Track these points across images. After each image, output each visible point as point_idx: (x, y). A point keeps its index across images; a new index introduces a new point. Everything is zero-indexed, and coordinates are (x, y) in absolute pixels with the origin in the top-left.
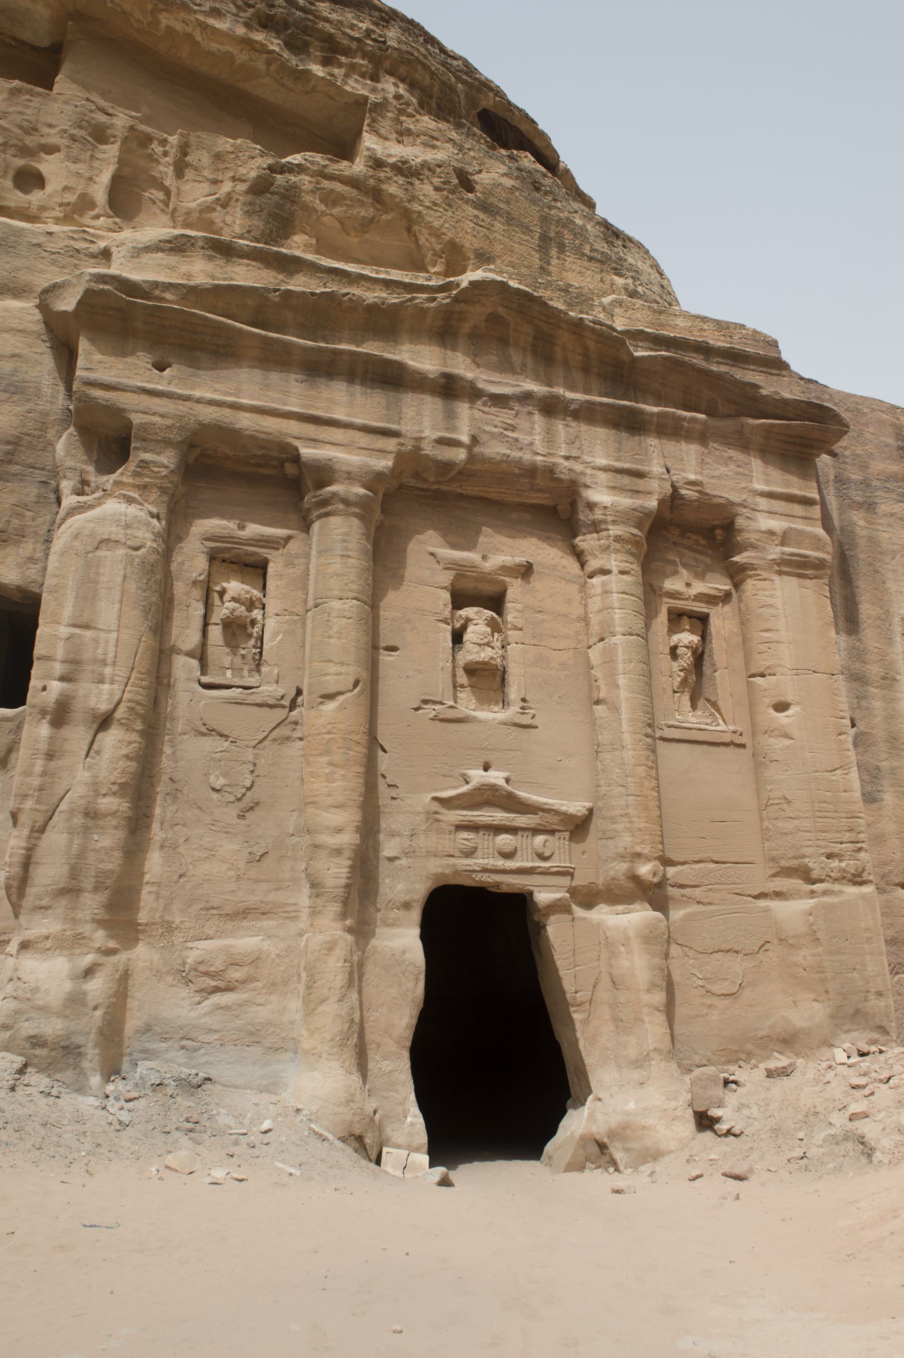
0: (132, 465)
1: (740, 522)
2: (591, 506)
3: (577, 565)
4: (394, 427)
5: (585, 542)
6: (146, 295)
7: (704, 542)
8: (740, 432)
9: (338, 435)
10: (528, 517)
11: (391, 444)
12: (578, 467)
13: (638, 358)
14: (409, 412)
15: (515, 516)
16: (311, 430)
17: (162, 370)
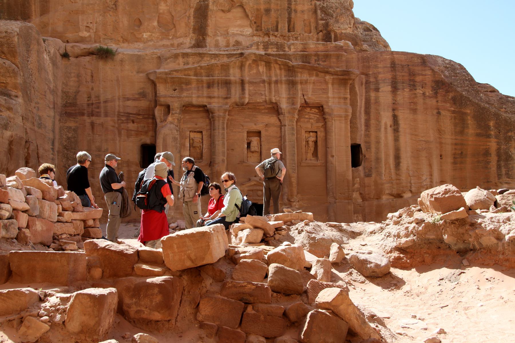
0: (170, 115)
1: (325, 106)
2: (281, 108)
3: (279, 123)
4: (229, 96)
5: (281, 117)
6: (170, 74)
7: (317, 111)
8: (325, 81)
9: (216, 100)
10: (267, 111)
11: (228, 101)
12: (278, 99)
13: (293, 66)
14: (233, 91)
15: (263, 111)
16: (209, 100)
17: (175, 90)
